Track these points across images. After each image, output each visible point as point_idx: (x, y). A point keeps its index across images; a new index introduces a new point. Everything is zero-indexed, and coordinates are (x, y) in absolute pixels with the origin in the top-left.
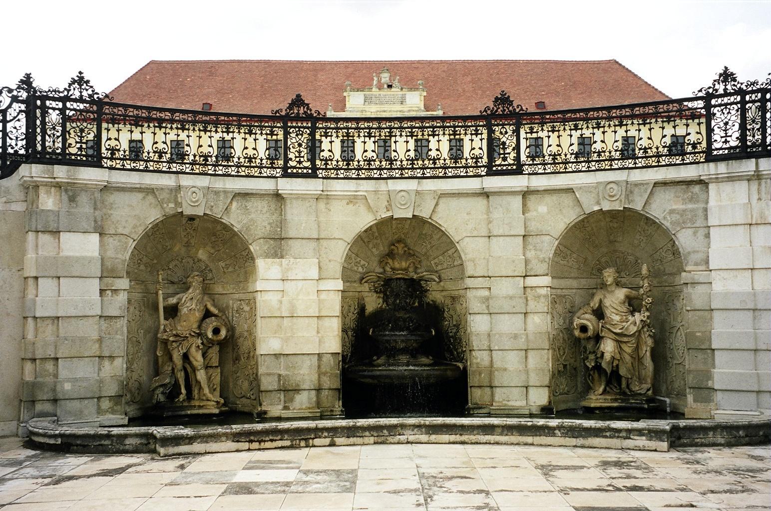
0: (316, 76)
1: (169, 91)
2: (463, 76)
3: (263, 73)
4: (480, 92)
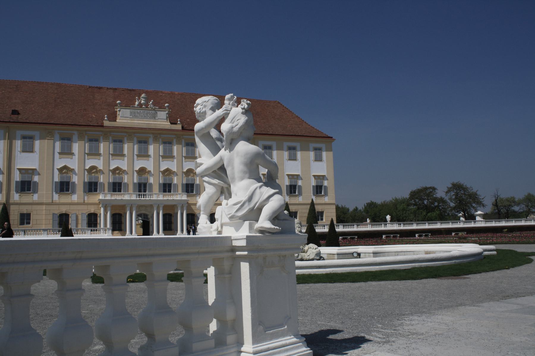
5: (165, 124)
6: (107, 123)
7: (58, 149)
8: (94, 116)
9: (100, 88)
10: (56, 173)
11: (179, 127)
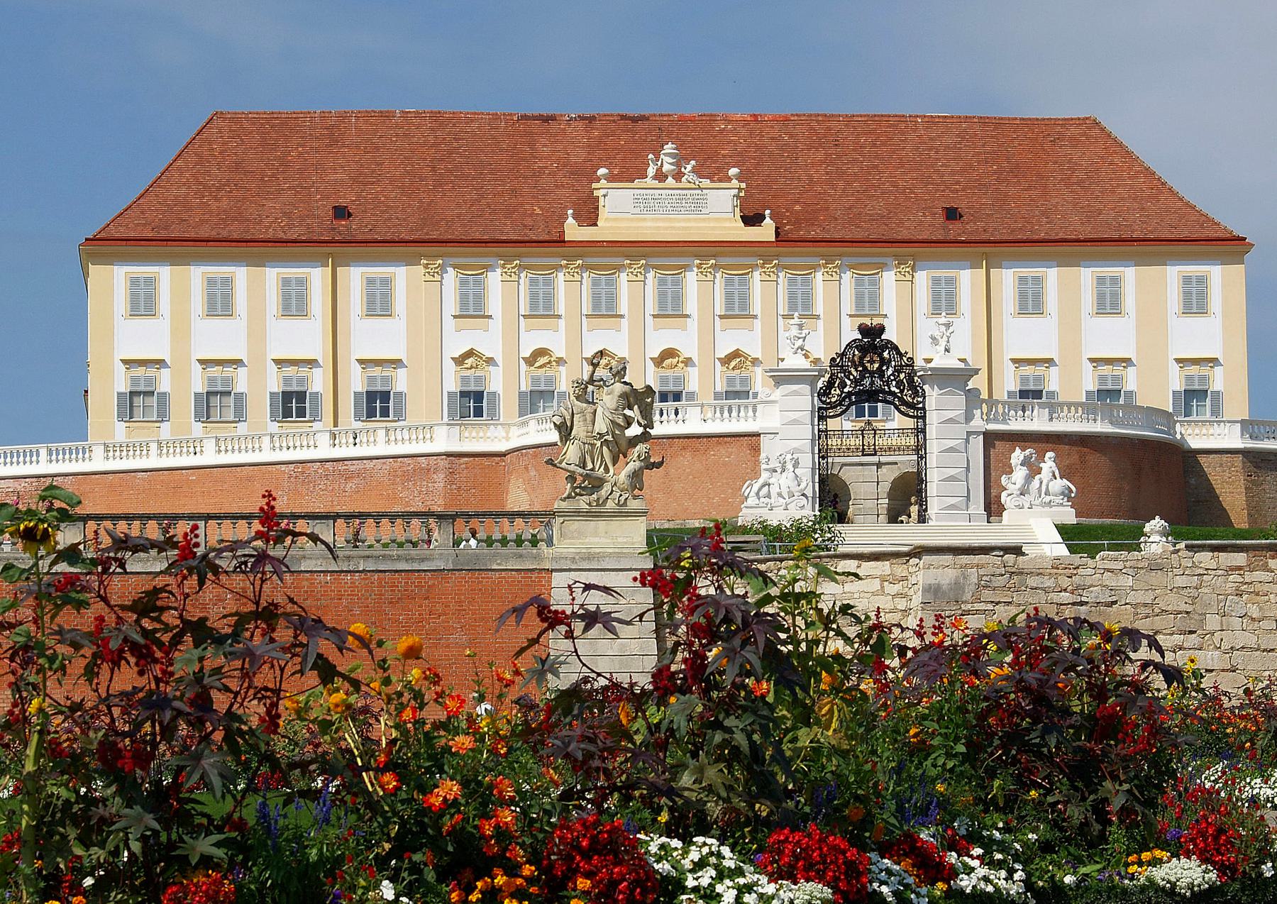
0: (532, 145)
1: (262, 179)
2: (809, 150)
3: (432, 140)
4: (841, 184)
5: (730, 228)
6: (573, 230)
7: (451, 305)
8: (538, 211)
9: (547, 119)
10: (450, 367)
11: (766, 231)
